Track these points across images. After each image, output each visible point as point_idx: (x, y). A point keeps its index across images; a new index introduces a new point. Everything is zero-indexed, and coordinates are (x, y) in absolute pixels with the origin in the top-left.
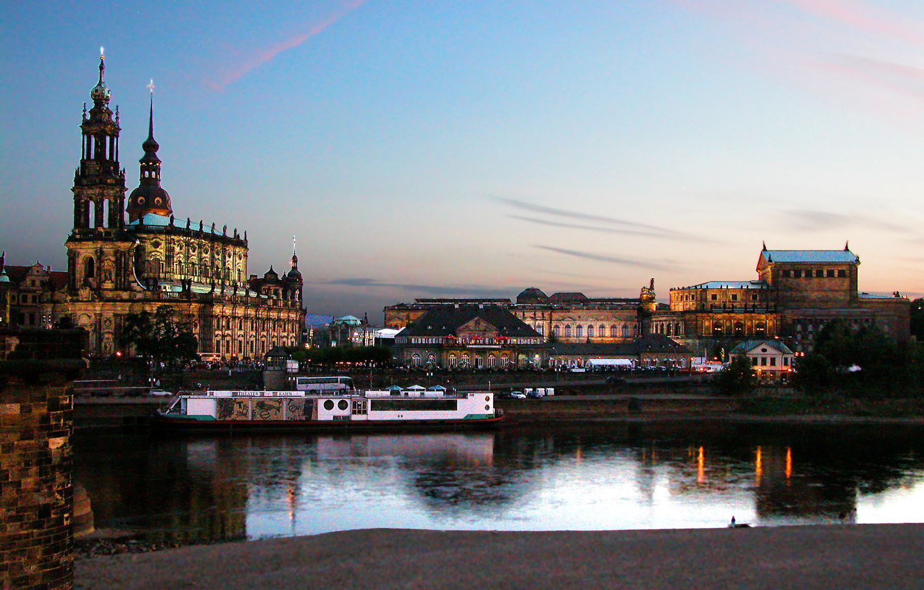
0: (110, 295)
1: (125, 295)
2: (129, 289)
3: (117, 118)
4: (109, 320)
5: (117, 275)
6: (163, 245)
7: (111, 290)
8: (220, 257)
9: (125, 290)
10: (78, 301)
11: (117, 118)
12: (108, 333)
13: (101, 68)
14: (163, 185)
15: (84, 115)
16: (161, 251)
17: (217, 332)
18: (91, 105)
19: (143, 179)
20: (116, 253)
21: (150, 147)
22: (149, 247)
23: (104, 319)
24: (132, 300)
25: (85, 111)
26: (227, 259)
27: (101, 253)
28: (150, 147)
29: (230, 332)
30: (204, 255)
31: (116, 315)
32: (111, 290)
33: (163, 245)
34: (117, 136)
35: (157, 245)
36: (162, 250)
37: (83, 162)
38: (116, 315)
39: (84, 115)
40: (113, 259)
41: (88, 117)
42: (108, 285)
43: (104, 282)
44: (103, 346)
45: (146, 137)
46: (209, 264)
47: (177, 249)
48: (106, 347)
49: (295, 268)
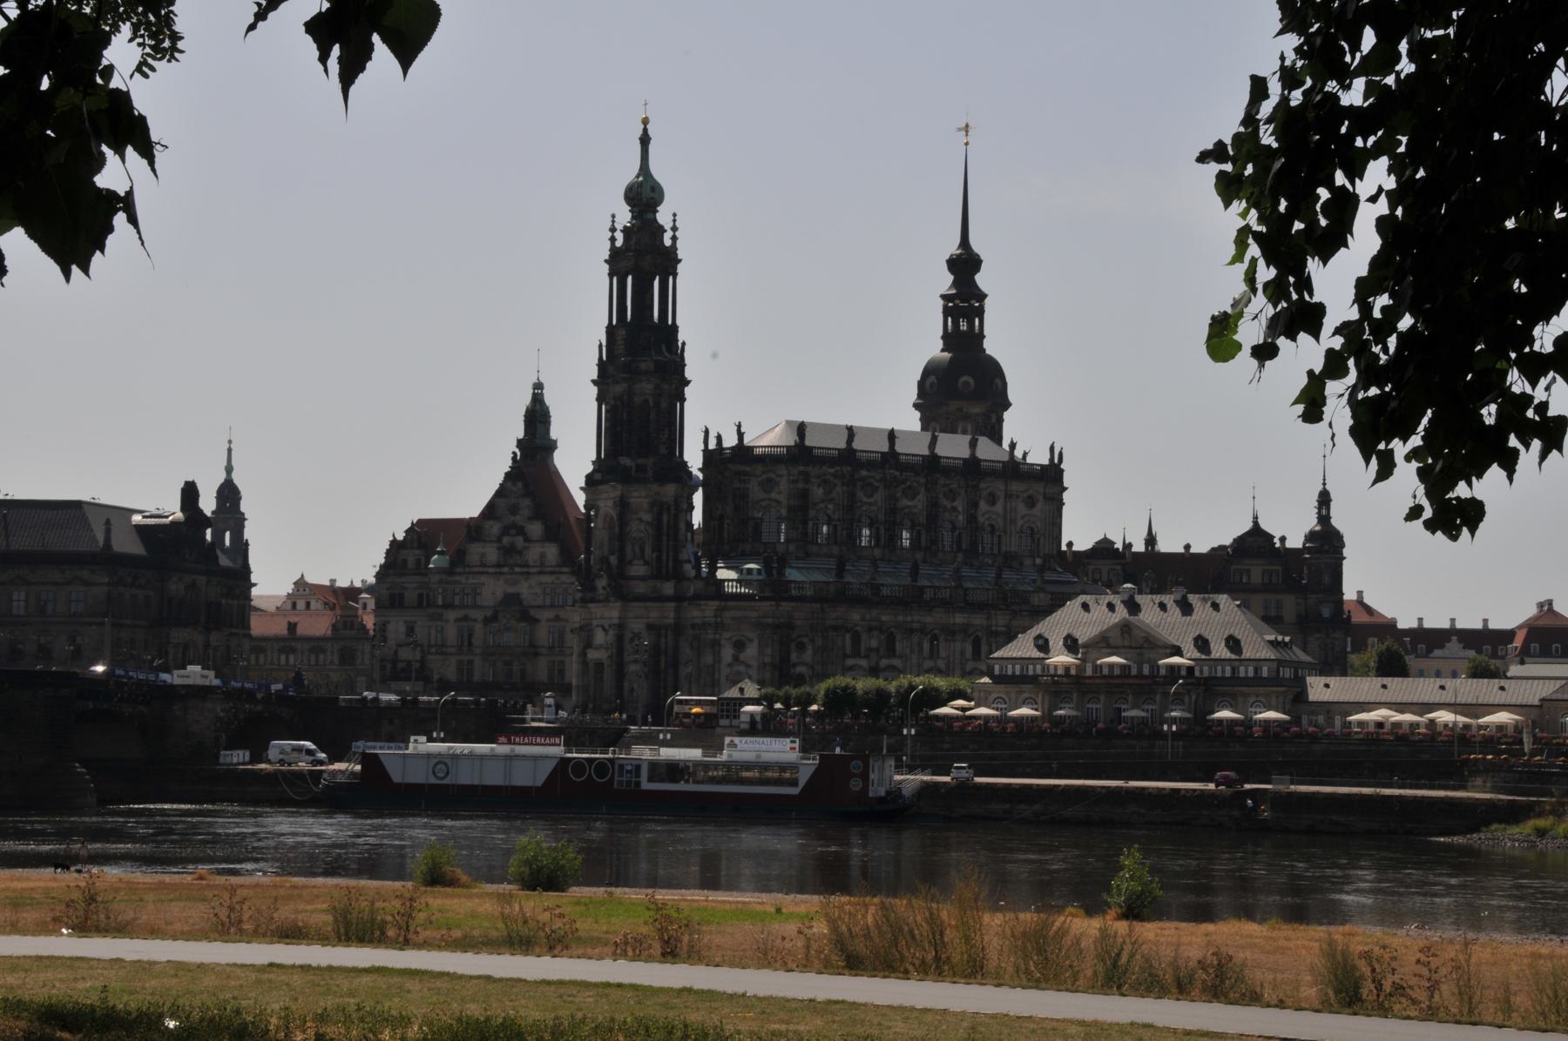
0: (641, 588)
1: (668, 588)
2: (678, 576)
3: (674, 238)
4: (637, 636)
5: (657, 548)
6: (784, 484)
7: (643, 579)
8: (959, 504)
9: (667, 578)
10: (593, 600)
11: (674, 238)
12: (636, 661)
13: (645, 140)
14: (991, 347)
15: (613, 239)
16: (781, 498)
17: (850, 662)
18: (625, 217)
19: (949, 340)
20: (653, 504)
21: (965, 265)
22: (755, 491)
23: (628, 636)
24: (678, 598)
25: (613, 230)
26: (983, 506)
27: (623, 505)
28: (965, 265)
29: (897, 662)
30: (905, 502)
31: (650, 627)
32: (643, 579)
33: (784, 484)
34: (675, 275)
35: (768, 485)
36: (782, 493)
37: (610, 330)
38: (650, 627)
39: (613, 239)
40: (647, 517)
41: (619, 243)
42: (638, 569)
43: (630, 563)
44: (626, 684)
45: (952, 247)
46: (923, 519)
47: (818, 492)
48: (632, 690)
49: (1324, 519)
